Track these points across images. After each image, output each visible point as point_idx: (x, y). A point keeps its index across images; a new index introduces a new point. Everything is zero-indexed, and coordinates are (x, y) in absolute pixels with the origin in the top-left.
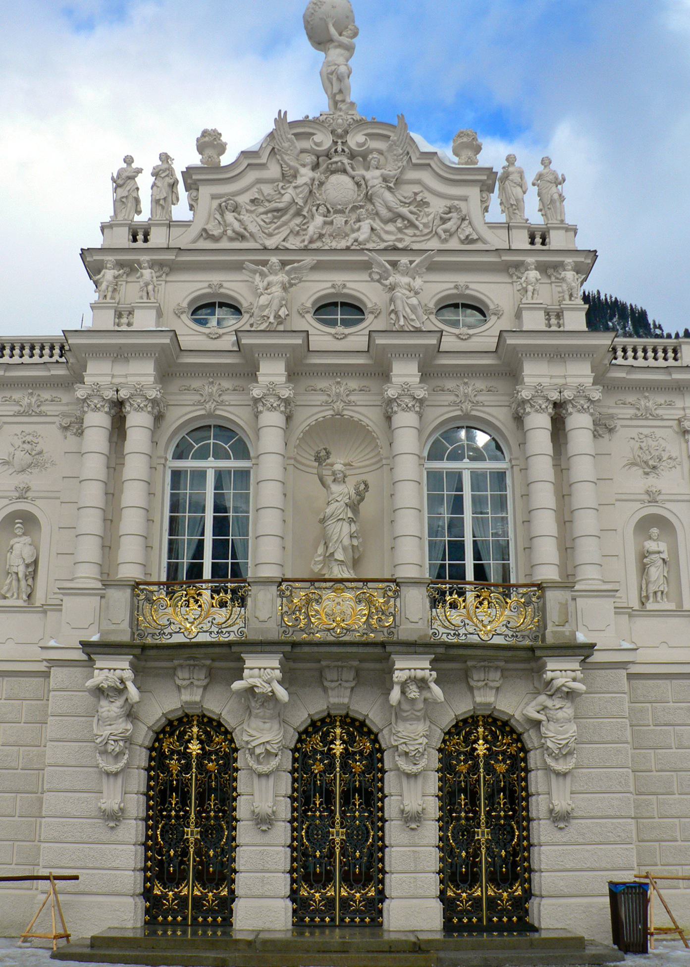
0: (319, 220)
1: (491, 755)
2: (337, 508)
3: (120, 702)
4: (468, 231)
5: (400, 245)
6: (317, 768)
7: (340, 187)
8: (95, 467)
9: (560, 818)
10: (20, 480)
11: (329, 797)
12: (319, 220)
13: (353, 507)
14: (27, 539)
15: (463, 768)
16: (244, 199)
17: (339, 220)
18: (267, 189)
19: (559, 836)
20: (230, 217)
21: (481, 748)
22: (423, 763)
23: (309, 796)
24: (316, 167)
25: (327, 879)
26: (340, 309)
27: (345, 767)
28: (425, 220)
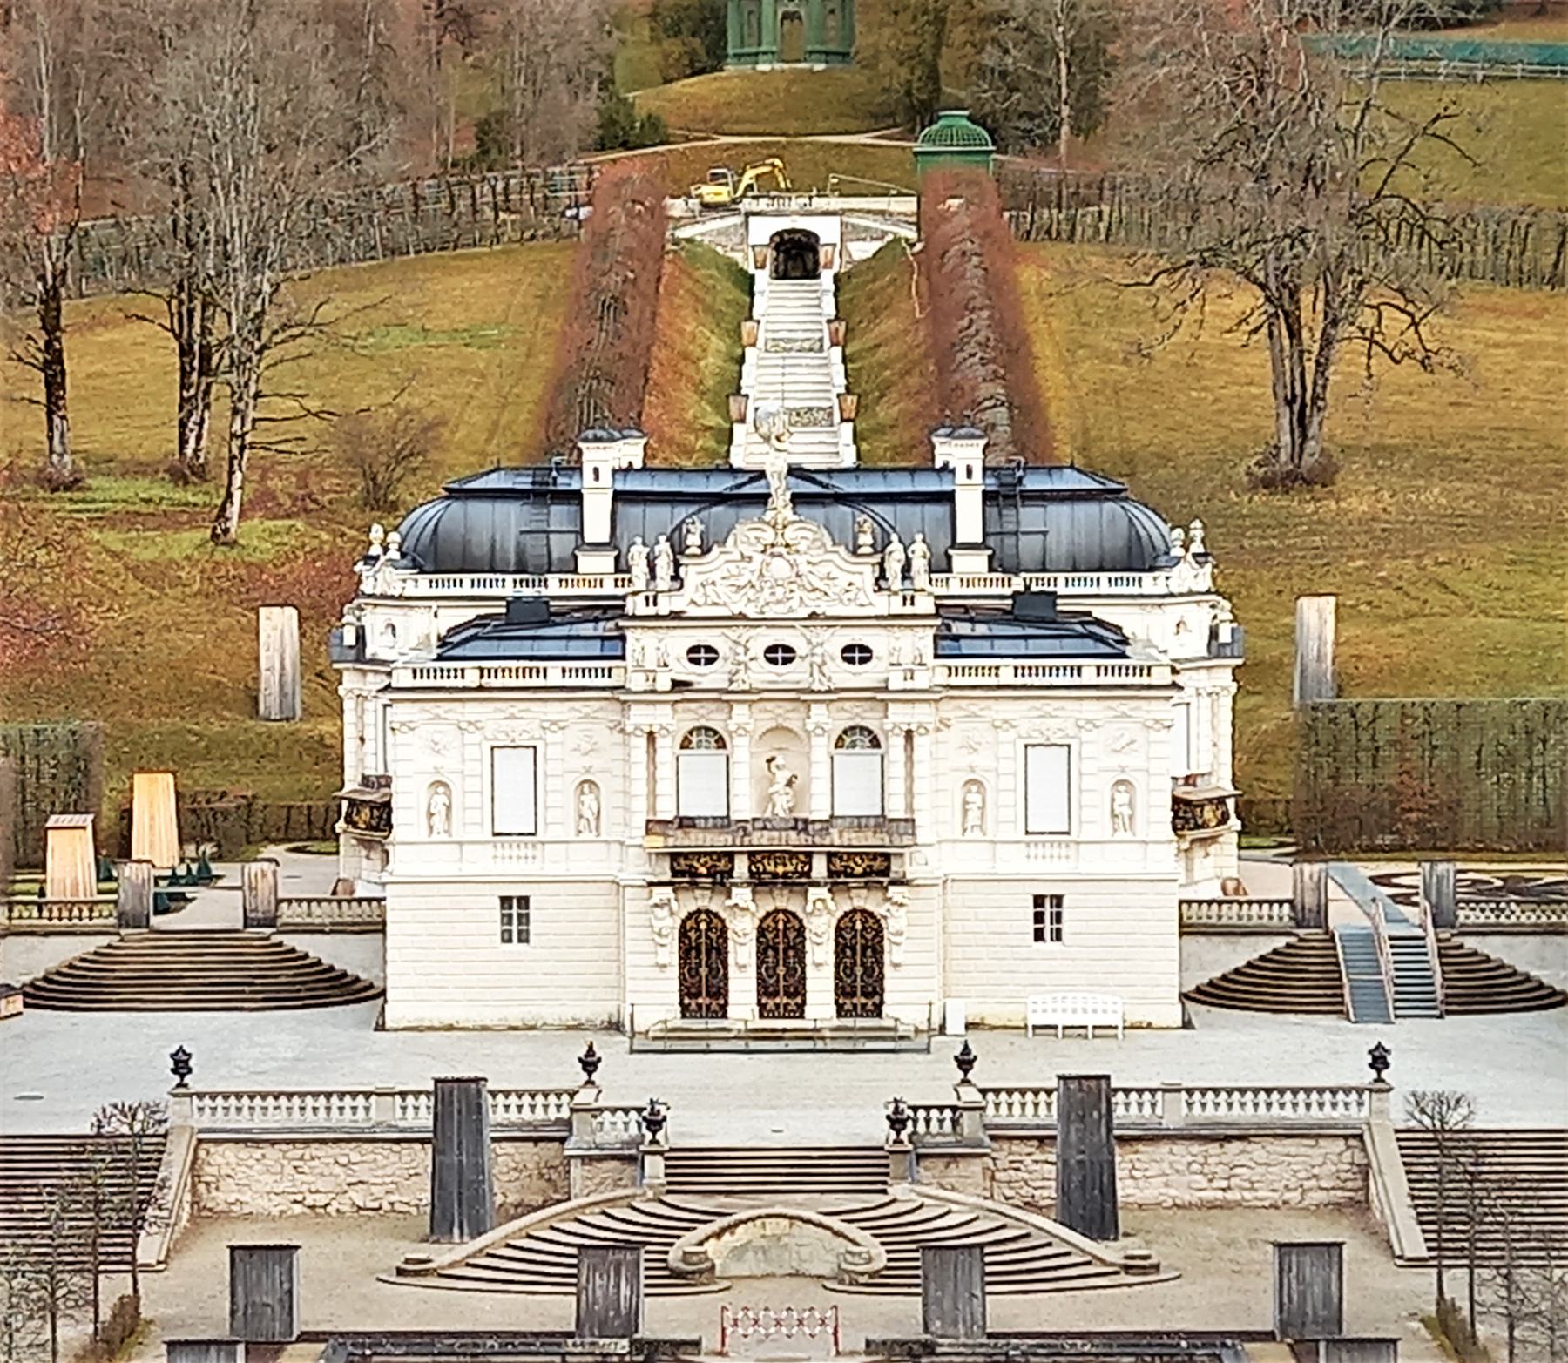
0: (767, 592)
1: (864, 928)
2: (780, 785)
3: (666, 909)
4: (862, 599)
5: (819, 611)
6: (770, 936)
7: (780, 568)
8: (640, 771)
9: (896, 965)
10: (587, 761)
11: (776, 950)
12: (767, 592)
13: (789, 784)
14: (592, 796)
15: (848, 936)
16: (715, 576)
17: (779, 592)
18: (732, 566)
19: (896, 974)
20: (709, 589)
21: (859, 926)
22: (825, 937)
23: (764, 948)
24: (764, 552)
25: (775, 994)
26: (780, 654)
27: (785, 936)
28: (837, 590)
